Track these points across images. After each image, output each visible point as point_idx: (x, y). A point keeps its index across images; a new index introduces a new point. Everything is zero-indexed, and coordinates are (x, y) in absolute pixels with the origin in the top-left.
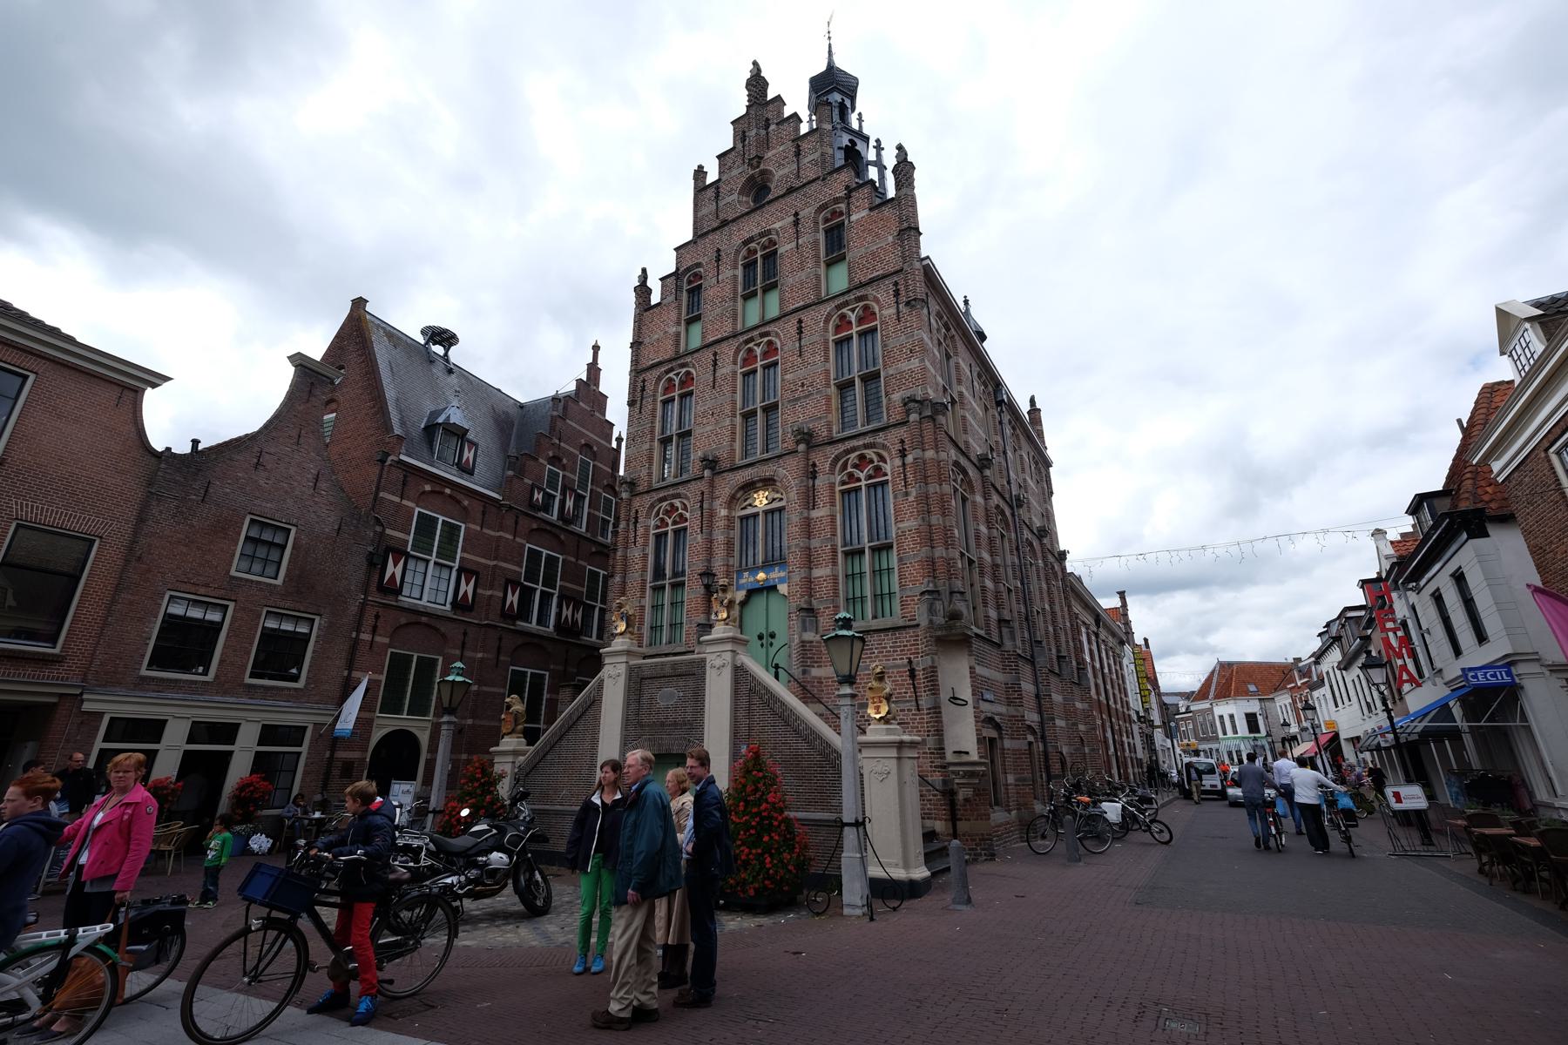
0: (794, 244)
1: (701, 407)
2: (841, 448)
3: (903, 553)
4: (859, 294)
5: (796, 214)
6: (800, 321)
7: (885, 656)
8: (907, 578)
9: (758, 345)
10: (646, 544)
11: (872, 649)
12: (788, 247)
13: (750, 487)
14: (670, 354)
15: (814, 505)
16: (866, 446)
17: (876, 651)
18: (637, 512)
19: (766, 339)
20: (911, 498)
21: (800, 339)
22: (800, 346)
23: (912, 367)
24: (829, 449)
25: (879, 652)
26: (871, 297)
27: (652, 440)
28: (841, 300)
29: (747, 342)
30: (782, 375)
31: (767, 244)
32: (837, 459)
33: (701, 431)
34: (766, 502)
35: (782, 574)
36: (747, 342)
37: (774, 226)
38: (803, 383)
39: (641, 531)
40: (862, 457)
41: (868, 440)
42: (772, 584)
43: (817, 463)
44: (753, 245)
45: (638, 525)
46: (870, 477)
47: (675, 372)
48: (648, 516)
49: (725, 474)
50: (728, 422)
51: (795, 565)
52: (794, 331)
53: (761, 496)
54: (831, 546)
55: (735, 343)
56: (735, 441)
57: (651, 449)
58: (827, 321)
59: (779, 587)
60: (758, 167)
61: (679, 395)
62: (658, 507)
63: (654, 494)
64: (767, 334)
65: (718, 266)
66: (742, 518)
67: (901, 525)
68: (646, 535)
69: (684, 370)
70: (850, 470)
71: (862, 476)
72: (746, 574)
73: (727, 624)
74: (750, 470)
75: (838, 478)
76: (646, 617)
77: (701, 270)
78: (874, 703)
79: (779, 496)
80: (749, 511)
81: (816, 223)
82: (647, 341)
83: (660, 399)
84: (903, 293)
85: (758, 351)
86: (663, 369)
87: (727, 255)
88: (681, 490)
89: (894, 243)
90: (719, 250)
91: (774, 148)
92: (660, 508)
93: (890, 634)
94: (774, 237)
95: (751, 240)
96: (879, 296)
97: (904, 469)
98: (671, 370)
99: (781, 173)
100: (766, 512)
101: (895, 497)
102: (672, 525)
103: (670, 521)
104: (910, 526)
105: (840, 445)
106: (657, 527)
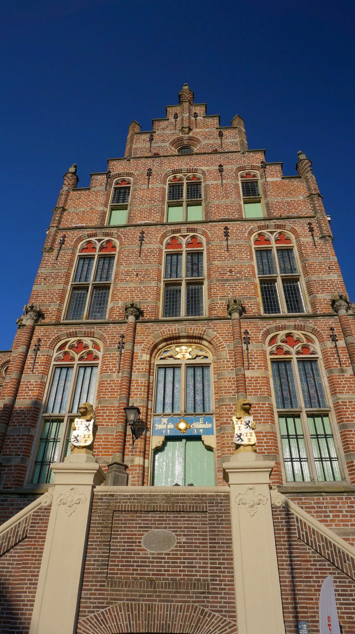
0: (219, 182)
1: (124, 267)
2: (273, 324)
4: (279, 224)
7: (342, 521)
9: (184, 236)
10: (45, 373)
11: (326, 512)
12: (215, 182)
14: (95, 223)
16: (296, 328)
17: (331, 514)
18: (39, 340)
19: (192, 234)
21: (227, 240)
22: (227, 245)
23: (333, 279)
24: (260, 322)
25: (334, 516)
26: (288, 228)
27: (66, 283)
28: (263, 223)
29: (174, 232)
30: (208, 260)
32: (267, 333)
33: (123, 286)
34: (190, 357)
36: (174, 232)
37: (201, 168)
39: (41, 358)
40: (289, 335)
42: (195, 433)
43: (250, 332)
44: (179, 175)
45: (39, 353)
46: (298, 353)
48: (52, 347)
49: (150, 324)
50: (153, 284)
52: (221, 233)
54: (269, 404)
55: (163, 230)
56: (159, 301)
57: (64, 291)
58: (250, 233)
59: (204, 438)
60: (188, 134)
61: (99, 255)
62: (68, 340)
63: (63, 328)
64: (194, 230)
65: (149, 179)
66: (160, 367)
67: (339, 396)
69: (107, 239)
70: (279, 343)
72: (165, 420)
73: (255, 451)
74: (177, 326)
75: (268, 349)
76: (33, 446)
77: (131, 179)
81: (237, 175)
83: (78, 254)
84: (315, 228)
85: (184, 241)
86: (87, 233)
87: (158, 174)
88: (96, 329)
89: (304, 201)
90: (150, 170)
91: (200, 128)
92: (67, 343)
93: (344, 497)
94: (199, 175)
95: (180, 171)
96: (296, 228)
99: (207, 142)
100: (188, 366)
102: (79, 360)
103: (77, 357)
106: (58, 359)
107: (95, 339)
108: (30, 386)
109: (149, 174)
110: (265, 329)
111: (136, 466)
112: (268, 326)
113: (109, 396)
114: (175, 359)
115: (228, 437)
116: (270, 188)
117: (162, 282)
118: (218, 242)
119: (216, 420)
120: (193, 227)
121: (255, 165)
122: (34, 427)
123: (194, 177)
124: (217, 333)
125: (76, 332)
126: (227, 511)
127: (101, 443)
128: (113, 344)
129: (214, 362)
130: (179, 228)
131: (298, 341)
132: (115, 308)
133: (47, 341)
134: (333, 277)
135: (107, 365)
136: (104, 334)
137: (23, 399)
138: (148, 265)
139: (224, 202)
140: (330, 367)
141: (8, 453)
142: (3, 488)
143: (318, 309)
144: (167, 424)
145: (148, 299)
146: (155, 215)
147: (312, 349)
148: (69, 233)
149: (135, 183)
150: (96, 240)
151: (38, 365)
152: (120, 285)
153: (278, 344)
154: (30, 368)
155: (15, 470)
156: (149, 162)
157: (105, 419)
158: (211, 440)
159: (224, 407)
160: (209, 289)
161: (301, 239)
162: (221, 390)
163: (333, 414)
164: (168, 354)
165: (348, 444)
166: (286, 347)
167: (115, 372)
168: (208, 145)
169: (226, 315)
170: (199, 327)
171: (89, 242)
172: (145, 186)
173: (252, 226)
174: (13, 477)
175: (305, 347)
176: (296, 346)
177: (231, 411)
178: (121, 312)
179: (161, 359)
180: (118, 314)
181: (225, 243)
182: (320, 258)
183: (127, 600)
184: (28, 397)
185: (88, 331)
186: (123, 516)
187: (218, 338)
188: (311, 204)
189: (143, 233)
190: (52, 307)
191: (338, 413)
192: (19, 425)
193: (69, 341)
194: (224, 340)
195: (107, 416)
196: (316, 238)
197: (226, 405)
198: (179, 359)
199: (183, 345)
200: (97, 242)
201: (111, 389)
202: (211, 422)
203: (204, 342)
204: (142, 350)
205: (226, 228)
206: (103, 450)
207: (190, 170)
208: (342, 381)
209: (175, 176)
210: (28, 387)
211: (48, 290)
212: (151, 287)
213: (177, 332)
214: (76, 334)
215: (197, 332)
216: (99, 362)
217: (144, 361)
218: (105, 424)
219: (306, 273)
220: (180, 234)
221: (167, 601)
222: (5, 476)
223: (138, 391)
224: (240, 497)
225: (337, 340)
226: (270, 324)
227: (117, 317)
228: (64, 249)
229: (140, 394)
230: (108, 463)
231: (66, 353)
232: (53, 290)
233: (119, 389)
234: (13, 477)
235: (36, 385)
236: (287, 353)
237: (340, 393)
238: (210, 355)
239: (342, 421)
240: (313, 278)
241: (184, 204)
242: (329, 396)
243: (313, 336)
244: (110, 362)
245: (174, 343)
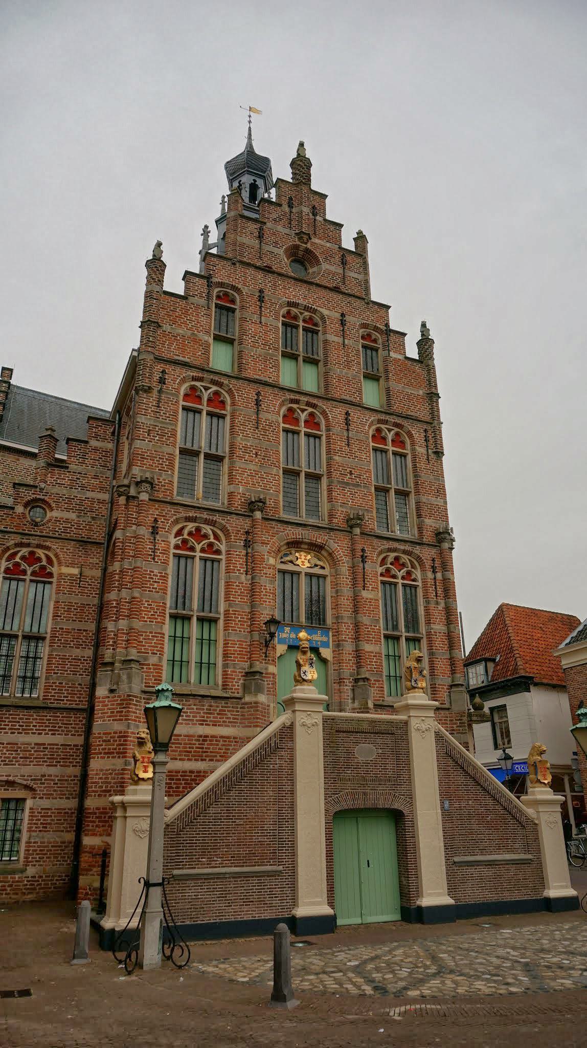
3: (435, 649)
4: (398, 422)
8: (438, 670)
10: (166, 563)
13: (295, 545)
15: (364, 586)
16: (404, 552)
18: (156, 520)
19: (310, 410)
20: (440, 608)
23: (439, 504)
24: (375, 541)
28: (383, 417)
29: (292, 401)
31: (308, 317)
32: (381, 552)
34: (309, 565)
35: (325, 639)
36: (292, 401)
38: (351, 471)
39: (161, 546)
41: (407, 547)
44: (294, 310)
45: (158, 537)
46: (403, 578)
49: (274, 523)
51: (348, 635)
52: (341, 418)
53: (303, 557)
59: (322, 650)
62: (185, 524)
64: (314, 406)
65: (261, 307)
68: (165, 552)
69: (214, 388)
78: (541, 772)
79: (319, 563)
80: (290, 567)
82: (167, 327)
86: (192, 374)
88: (217, 518)
90: (261, 291)
91: (320, 238)
94: (317, 318)
95: (296, 305)
96: (413, 432)
97: (435, 582)
98: (200, 379)
100: (307, 574)
101: (428, 602)
104: (440, 629)
105: (385, 542)
106: (177, 547)
107: (215, 529)
108: (154, 577)
109: (261, 299)
110: (380, 549)
111: (270, 674)
113: (239, 600)
114: (295, 565)
115: (346, 654)
116: (391, 368)
117: (281, 469)
118: (338, 430)
119: (333, 636)
120: (314, 402)
121: (379, 326)
122: (164, 624)
123: (311, 318)
124: (338, 546)
125: (196, 517)
126: (406, 733)
127: (236, 648)
128: (238, 539)
129: (331, 576)
130: (298, 398)
131: (404, 565)
132: (236, 494)
134: (439, 502)
135: (235, 564)
136: (227, 525)
137: (149, 591)
138: (268, 443)
139: (346, 373)
140: (428, 598)
141: (143, 651)
142: (145, 686)
143: (425, 536)
144: (290, 634)
145: (270, 490)
146: (271, 370)
147: (413, 576)
148: (169, 368)
149: (242, 308)
150: (201, 386)
151: (160, 553)
153: (388, 566)
154: (151, 555)
155: (154, 669)
156: (260, 275)
157: (238, 624)
158: (326, 653)
159: (343, 625)
160: (330, 491)
162: (341, 607)
163: (424, 642)
164: (288, 558)
165: (434, 669)
166: (394, 570)
167: (242, 574)
168: (329, 272)
169: (349, 529)
170: (321, 535)
171: (193, 388)
173: (373, 418)
174: (153, 676)
175: (409, 573)
176: (402, 571)
177: (349, 629)
178: (243, 500)
179: (281, 562)
180: (240, 503)
181: (345, 433)
182: (431, 477)
183: (351, 789)
184: (154, 590)
185: (209, 519)
186: (341, 735)
187: (339, 551)
188: (429, 404)
190: (164, 477)
191: (430, 641)
192: (150, 621)
194: (344, 555)
195: (239, 621)
196: (430, 451)
197: (345, 623)
198: (298, 565)
199: (301, 551)
201: (241, 593)
202: (328, 636)
203: (323, 552)
204: (268, 552)
205: (347, 414)
206: (239, 656)
207: (308, 308)
208: (436, 613)
209: (290, 310)
210: (152, 578)
211: (155, 451)
212: (272, 474)
213: (300, 537)
214: (195, 520)
215: (320, 541)
216: (223, 557)
217: (271, 565)
218: (238, 630)
219: (417, 492)
220: (297, 406)
221: (375, 790)
222: (145, 674)
223: (268, 599)
224: (417, 725)
225: (436, 572)
226: (384, 545)
227: (239, 507)
228: (167, 393)
229: (269, 602)
230: (245, 669)
231: (185, 542)
232: (161, 452)
233: (249, 593)
234: (153, 676)
235: (160, 576)
236: (394, 577)
237: (433, 623)
238: (327, 566)
239: (432, 649)
240: (424, 499)
241: (301, 359)
242: (424, 624)
243: (416, 563)
244: (236, 561)
245: (294, 547)
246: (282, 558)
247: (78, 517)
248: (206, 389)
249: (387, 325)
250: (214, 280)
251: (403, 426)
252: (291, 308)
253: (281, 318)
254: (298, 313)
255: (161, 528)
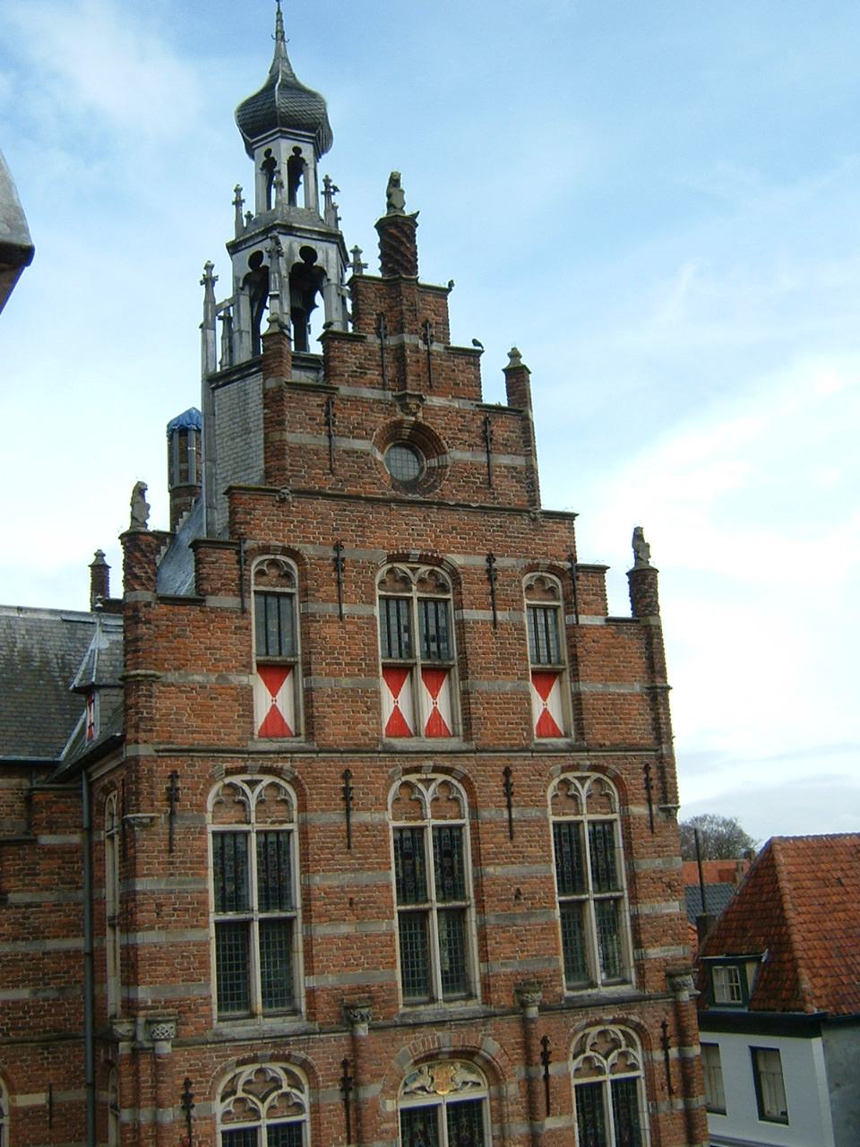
5: (491, 558)
6: (507, 772)
16: (614, 1022)
18: (188, 1083)
21: (509, 807)
22: (510, 820)
47: (247, 777)
64: (447, 771)
65: (339, 583)
71: (607, 1064)
79: (473, 1078)
85: (428, 796)
95: (404, 558)
112: (577, 1024)
133: (202, 1082)
136: (310, 1058)
148: (182, 766)
152: (322, 930)
161: (631, 807)
172: (331, 608)
189: (346, 776)
193: (241, 1073)
196: (654, 807)
200: (245, 787)
203: (476, 1059)
219: (634, 899)
220: (418, 776)
246: (406, 1085)
247: (35, 993)
248: (252, 784)
249: (572, 558)
250: (249, 544)
251: (607, 768)
252: (395, 565)
253: (379, 592)
254: (408, 571)
255: (197, 1094)
